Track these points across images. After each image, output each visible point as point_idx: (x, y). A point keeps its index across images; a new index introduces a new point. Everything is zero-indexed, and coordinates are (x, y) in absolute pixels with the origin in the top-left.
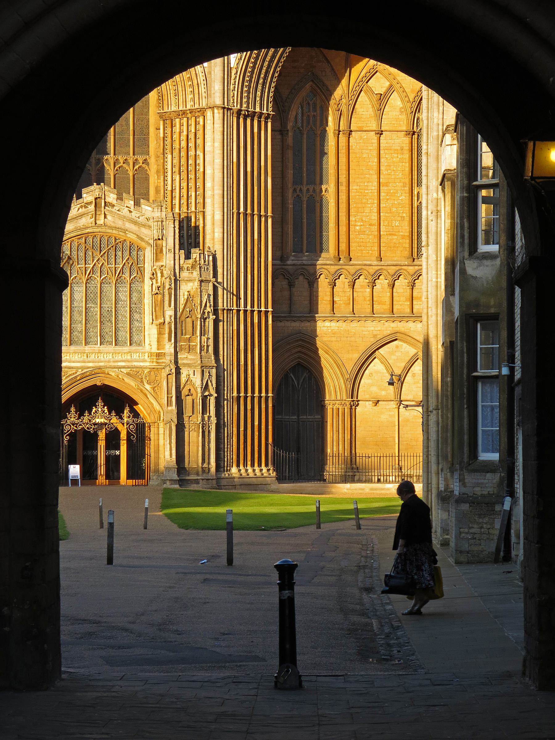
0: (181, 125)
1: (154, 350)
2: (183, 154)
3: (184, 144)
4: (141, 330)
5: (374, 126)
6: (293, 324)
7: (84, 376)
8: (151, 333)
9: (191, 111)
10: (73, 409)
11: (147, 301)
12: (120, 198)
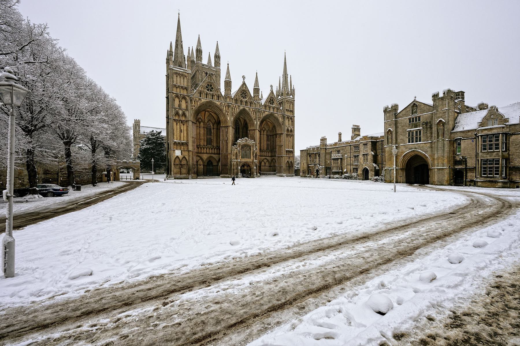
8: (252, 157)
11: (252, 153)
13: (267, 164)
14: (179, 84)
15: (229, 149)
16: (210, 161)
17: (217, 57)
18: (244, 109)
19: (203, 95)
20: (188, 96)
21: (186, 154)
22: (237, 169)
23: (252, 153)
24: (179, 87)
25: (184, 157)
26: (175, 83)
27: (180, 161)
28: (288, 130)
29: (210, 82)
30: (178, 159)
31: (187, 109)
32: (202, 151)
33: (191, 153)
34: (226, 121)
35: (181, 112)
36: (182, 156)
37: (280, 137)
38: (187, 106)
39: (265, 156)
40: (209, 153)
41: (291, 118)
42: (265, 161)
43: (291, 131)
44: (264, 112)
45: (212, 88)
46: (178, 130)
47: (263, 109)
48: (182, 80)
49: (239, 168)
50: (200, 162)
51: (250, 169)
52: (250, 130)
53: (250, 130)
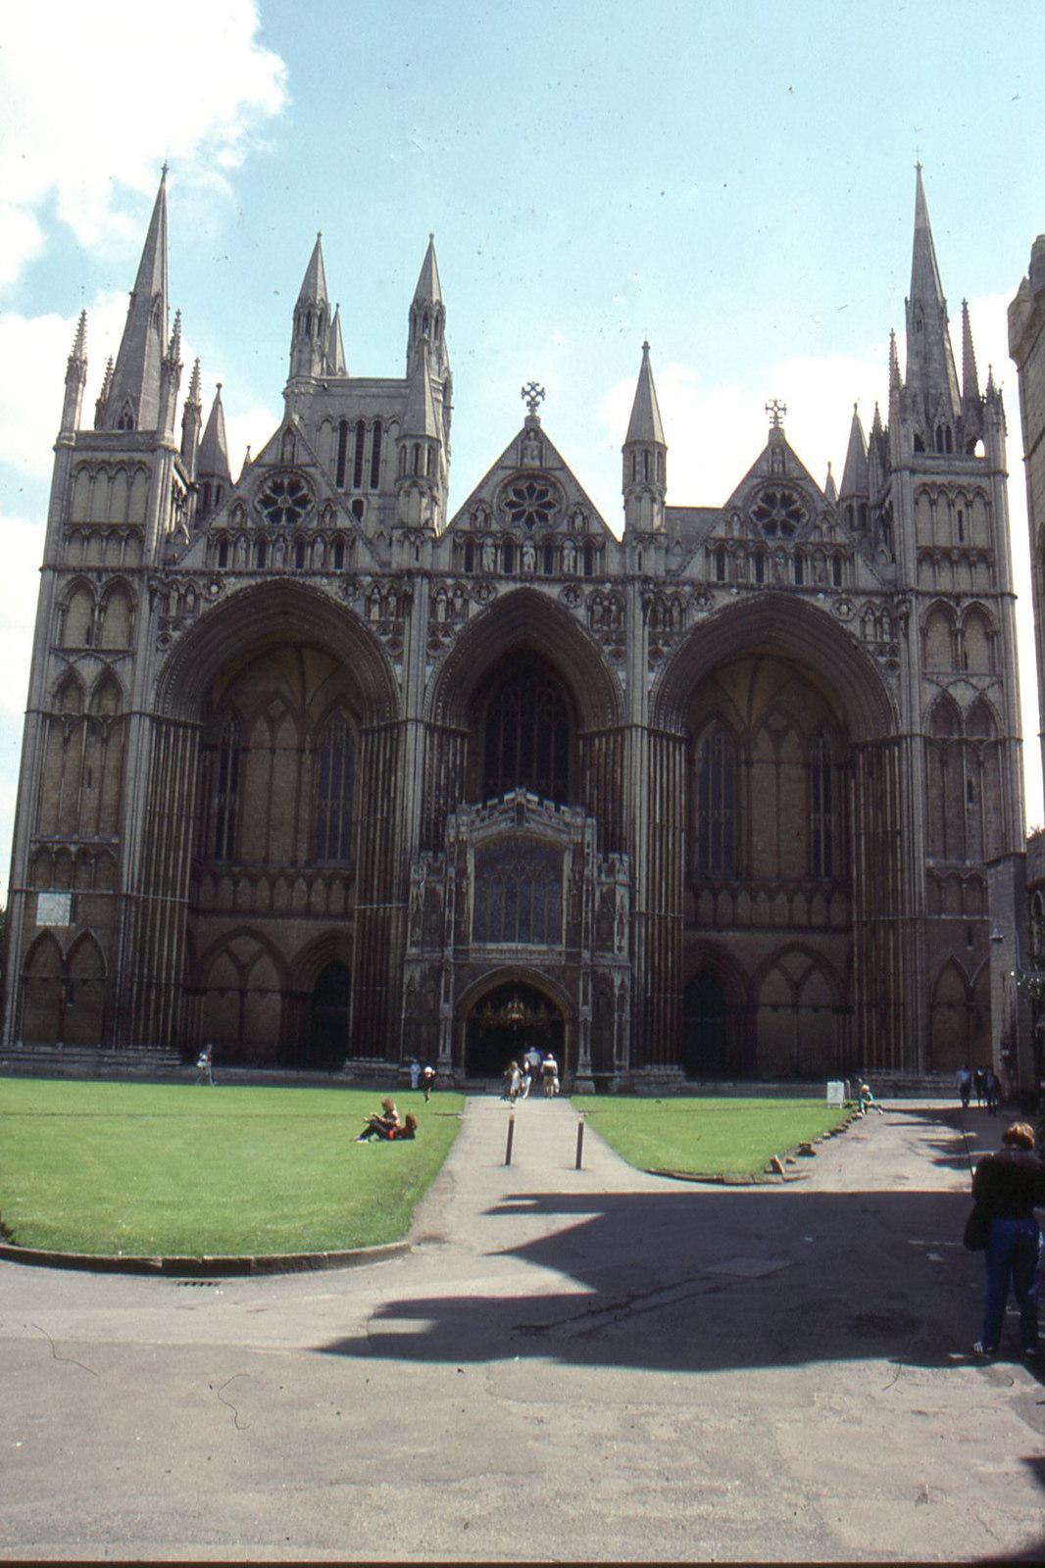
0: (600, 744)
2: (602, 770)
3: (602, 760)
14: (99, 517)
18: (524, 601)
19: (243, 556)
26: (78, 517)
27: (66, 966)
28: (945, 706)
31: (128, 653)
35: (89, 671)
41: (977, 613)
45: (303, 502)
47: (698, 567)
49: (447, 1009)
52: (589, 739)
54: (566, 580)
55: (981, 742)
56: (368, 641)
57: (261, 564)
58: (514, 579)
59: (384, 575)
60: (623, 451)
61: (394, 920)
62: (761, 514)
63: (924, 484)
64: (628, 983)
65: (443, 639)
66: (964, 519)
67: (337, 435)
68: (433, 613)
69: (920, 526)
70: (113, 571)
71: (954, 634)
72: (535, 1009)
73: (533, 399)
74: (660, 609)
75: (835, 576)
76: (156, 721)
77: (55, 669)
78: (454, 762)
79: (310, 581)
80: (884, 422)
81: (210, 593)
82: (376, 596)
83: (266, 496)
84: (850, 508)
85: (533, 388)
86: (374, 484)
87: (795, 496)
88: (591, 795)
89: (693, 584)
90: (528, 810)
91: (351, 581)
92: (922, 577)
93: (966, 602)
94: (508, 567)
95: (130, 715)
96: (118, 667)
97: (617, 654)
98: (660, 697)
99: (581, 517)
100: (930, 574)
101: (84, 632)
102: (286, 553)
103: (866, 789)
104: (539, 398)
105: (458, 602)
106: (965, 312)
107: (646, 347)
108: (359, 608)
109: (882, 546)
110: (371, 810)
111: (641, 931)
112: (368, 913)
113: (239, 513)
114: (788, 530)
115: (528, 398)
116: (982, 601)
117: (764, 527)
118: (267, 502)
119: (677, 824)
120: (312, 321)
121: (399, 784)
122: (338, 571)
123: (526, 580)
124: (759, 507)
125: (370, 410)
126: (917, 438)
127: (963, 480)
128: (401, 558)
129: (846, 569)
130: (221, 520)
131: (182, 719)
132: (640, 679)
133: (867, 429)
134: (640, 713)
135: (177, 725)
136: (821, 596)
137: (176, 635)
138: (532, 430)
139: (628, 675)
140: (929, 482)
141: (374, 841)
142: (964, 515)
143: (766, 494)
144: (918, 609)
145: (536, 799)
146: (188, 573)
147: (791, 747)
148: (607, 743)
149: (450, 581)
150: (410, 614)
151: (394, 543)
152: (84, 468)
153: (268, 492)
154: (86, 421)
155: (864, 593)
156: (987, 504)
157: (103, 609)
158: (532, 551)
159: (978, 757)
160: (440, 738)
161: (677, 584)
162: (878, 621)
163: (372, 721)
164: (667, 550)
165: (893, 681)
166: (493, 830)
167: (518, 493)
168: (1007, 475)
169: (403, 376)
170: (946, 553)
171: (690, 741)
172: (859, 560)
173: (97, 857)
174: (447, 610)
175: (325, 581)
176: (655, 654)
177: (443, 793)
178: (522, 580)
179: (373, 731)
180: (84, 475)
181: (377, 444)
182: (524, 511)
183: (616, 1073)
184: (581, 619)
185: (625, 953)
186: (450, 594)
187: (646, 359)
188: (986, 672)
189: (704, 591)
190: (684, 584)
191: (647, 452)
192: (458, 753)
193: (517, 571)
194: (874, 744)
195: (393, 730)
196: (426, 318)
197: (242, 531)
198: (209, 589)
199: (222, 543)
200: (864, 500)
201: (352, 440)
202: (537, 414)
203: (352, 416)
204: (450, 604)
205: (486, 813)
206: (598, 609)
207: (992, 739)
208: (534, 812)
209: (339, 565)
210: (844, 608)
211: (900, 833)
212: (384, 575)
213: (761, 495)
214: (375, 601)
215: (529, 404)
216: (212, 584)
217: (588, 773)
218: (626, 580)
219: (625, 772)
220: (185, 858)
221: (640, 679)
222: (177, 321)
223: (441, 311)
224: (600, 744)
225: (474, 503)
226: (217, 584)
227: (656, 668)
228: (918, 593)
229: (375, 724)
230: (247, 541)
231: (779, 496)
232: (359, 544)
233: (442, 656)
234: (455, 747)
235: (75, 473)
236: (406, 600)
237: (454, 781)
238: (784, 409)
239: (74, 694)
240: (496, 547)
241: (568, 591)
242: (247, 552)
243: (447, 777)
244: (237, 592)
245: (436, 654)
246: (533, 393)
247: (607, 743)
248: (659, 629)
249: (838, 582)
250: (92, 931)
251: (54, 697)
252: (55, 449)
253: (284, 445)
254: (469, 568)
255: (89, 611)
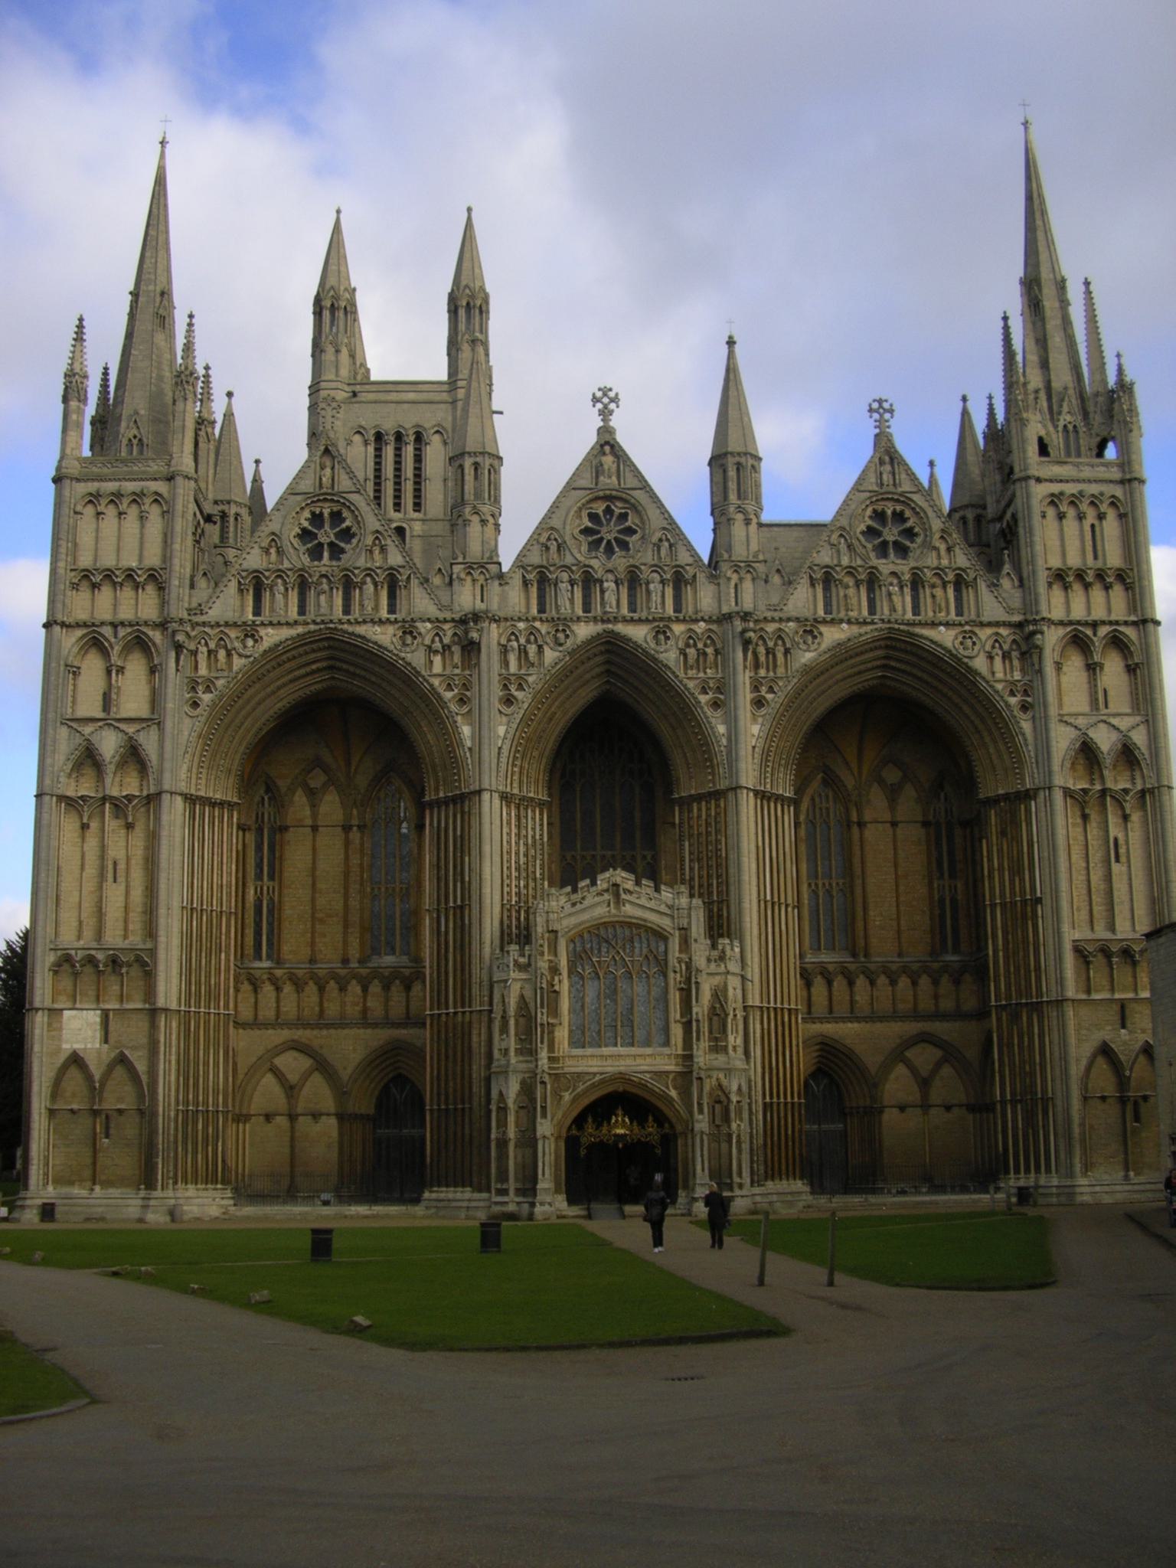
0: (699, 810)
1: (680, 1052)
2: (703, 839)
3: (703, 829)
4: (666, 1030)
5: (887, 817)
6: (814, 1026)
7: (602, 1082)
9: (710, 794)
10: (590, 1120)
12: (638, 883)
13: (948, 1085)
14: (108, 561)
15: (477, 973)
16: (400, 1080)
17: (467, 308)
19: (285, 603)
20: (162, 625)
21: (132, 1034)
22: (528, 1140)
23: (675, 998)
24: (109, 575)
25: (122, 1060)
26: (85, 561)
28: (1087, 752)
29: (321, 496)
30: (74, 1072)
31: (154, 719)
32: (332, 1009)
33: (169, 1032)
34: (452, 759)
35: (109, 745)
36: (108, 1053)
37: (1011, 827)
38: (156, 699)
39: (916, 1015)
40: (388, 1023)
41: (1117, 642)
42: (924, 1057)
43: (1128, 755)
44: (810, 629)
45: (347, 535)
46: (91, 871)
47: (803, 600)
48: (131, 522)
50: (318, 1093)
51: (668, 1141)
52: (687, 802)
53: (687, 802)
54: (654, 620)
55: (1126, 791)
56: (430, 702)
57: (302, 611)
58: (595, 620)
59: (445, 621)
60: (710, 464)
61: (475, 1025)
62: (870, 532)
63: (1053, 495)
64: (745, 1088)
65: (516, 694)
66: (1098, 533)
67: (371, 449)
68: (506, 663)
69: (1053, 542)
70: (131, 625)
71: (1092, 668)
72: (642, 1124)
73: (606, 407)
74: (762, 650)
75: (956, 607)
76: (190, 799)
77: (65, 743)
78: (533, 837)
79: (361, 630)
80: (1000, 417)
81: (245, 647)
82: (437, 645)
83: (304, 530)
84: (964, 519)
85: (605, 395)
86: (417, 507)
87: (908, 513)
88: (691, 869)
89: (797, 620)
90: (627, 891)
91: (409, 630)
92: (1053, 601)
93: (1103, 630)
94: (587, 608)
95: (159, 794)
96: (142, 738)
97: (716, 705)
98: (766, 754)
99: (666, 544)
100: (1062, 600)
101: (100, 698)
102: (331, 597)
103: (1000, 851)
104: (612, 406)
105: (532, 649)
106: (1088, 293)
107: (731, 343)
108: (416, 658)
109: (1007, 568)
110: (442, 895)
111: (756, 1028)
112: (444, 1018)
113: (273, 551)
114: (902, 551)
115: (599, 406)
116: (1122, 629)
117: (875, 549)
118: (305, 535)
119: (790, 901)
120: (334, 309)
121: (475, 866)
122: (392, 617)
123: (608, 621)
124: (869, 528)
125: (408, 419)
126: (1041, 440)
127: (1094, 489)
128: (466, 598)
129: (969, 596)
130: (254, 560)
131: (218, 796)
132: (747, 737)
133: (980, 425)
134: (748, 774)
135: (213, 804)
136: (942, 628)
137: (207, 698)
138: (607, 443)
139: (729, 730)
140: (1056, 492)
141: (447, 933)
142: (1097, 529)
143: (875, 511)
144: (1052, 639)
145: (633, 877)
146: (218, 625)
147: (909, 792)
148: (708, 809)
149: (521, 625)
150: (478, 664)
151: (455, 583)
152: (90, 502)
153: (306, 524)
154: (86, 452)
155: (990, 624)
156: (1122, 516)
157: (121, 670)
158: (613, 585)
159: (1123, 808)
160: (518, 807)
161: (781, 620)
162: (1006, 656)
163: (437, 790)
164: (766, 581)
165: (1026, 726)
166: (585, 916)
167: (593, 517)
168: (1142, 482)
169: (442, 375)
170: (1080, 575)
171: (796, 802)
172: (982, 586)
173: (130, 966)
174: (519, 659)
175: (377, 629)
176: (759, 703)
177: (524, 874)
178: (603, 621)
179: (438, 803)
180: (90, 511)
181: (418, 459)
182: (602, 539)
183: (737, 1192)
184: (672, 664)
185: (740, 1050)
186: (522, 641)
187: (731, 355)
188: (1128, 711)
189: (810, 629)
190: (789, 620)
191: (739, 466)
192: (537, 825)
193: (597, 610)
194: (1006, 797)
195: (464, 801)
196: (467, 308)
197: (280, 574)
198: (243, 642)
199: (257, 586)
200: (979, 511)
201: (389, 452)
202: (615, 422)
203: (389, 426)
204: (523, 652)
205: (574, 897)
206: (691, 652)
207: (1139, 787)
208: (631, 893)
209: (392, 609)
210: (969, 642)
211: (1039, 901)
212: (445, 621)
213: (869, 512)
214: (436, 652)
215: (601, 413)
216: (246, 636)
217: (687, 844)
218: (725, 618)
219: (730, 841)
220: (227, 959)
221: (747, 737)
222: (190, 325)
223: (486, 299)
224: (699, 810)
225: (546, 536)
226: (253, 636)
227: (760, 720)
228: (1051, 622)
229: (441, 795)
230: (285, 583)
231: (889, 512)
232: (414, 582)
233: (518, 712)
234: (534, 819)
235: (79, 508)
236: (471, 649)
237: (535, 858)
238: (891, 411)
239: (89, 771)
240: (572, 582)
241: (662, 632)
242: (286, 596)
243: (526, 855)
244: (277, 646)
245: (509, 711)
246: (606, 400)
247: (708, 809)
248: (762, 672)
249: (959, 613)
250: (126, 1052)
251: (69, 776)
252: (57, 480)
253: (322, 469)
254: (542, 610)
255: (102, 673)
